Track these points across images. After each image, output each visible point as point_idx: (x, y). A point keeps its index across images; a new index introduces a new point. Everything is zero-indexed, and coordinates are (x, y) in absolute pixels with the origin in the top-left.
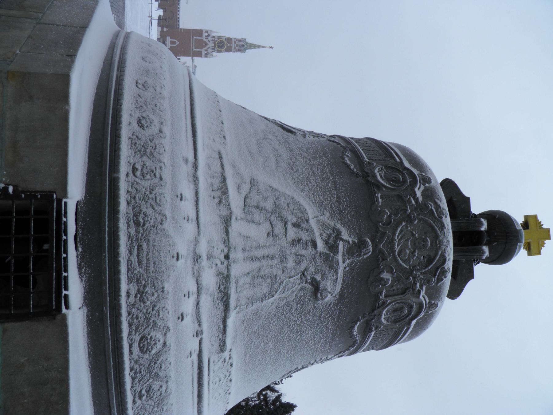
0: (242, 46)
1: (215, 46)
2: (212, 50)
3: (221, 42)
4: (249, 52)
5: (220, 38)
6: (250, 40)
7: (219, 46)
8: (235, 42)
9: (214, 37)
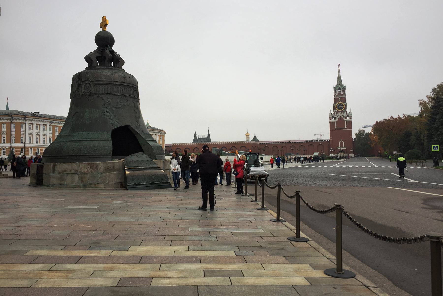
0: (340, 91)
1: (342, 112)
2: (345, 114)
3: (338, 106)
4: (344, 84)
5: (335, 108)
6: (335, 84)
7: (341, 108)
8: (337, 96)
9: (334, 113)
